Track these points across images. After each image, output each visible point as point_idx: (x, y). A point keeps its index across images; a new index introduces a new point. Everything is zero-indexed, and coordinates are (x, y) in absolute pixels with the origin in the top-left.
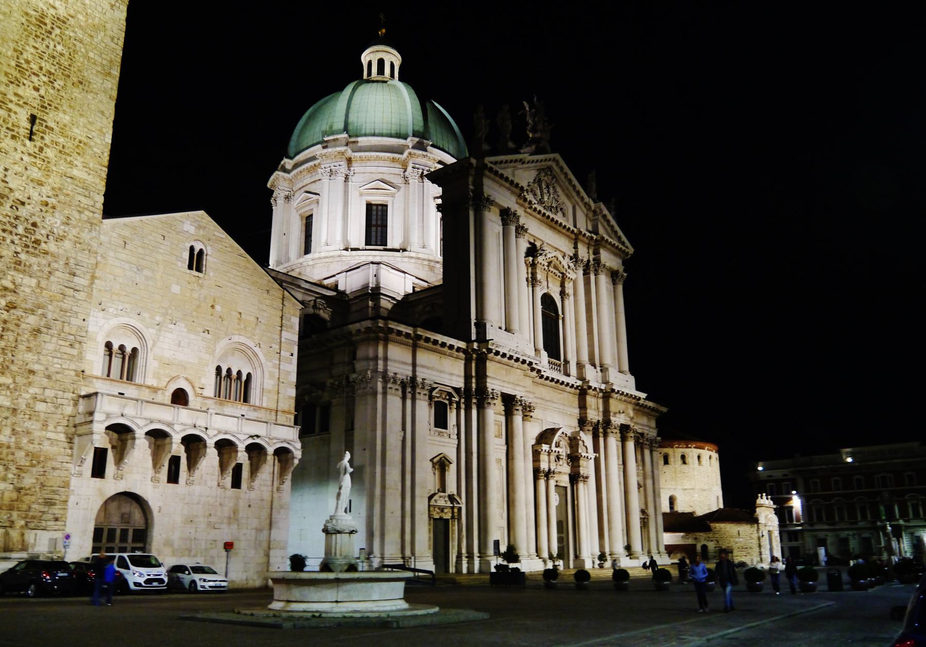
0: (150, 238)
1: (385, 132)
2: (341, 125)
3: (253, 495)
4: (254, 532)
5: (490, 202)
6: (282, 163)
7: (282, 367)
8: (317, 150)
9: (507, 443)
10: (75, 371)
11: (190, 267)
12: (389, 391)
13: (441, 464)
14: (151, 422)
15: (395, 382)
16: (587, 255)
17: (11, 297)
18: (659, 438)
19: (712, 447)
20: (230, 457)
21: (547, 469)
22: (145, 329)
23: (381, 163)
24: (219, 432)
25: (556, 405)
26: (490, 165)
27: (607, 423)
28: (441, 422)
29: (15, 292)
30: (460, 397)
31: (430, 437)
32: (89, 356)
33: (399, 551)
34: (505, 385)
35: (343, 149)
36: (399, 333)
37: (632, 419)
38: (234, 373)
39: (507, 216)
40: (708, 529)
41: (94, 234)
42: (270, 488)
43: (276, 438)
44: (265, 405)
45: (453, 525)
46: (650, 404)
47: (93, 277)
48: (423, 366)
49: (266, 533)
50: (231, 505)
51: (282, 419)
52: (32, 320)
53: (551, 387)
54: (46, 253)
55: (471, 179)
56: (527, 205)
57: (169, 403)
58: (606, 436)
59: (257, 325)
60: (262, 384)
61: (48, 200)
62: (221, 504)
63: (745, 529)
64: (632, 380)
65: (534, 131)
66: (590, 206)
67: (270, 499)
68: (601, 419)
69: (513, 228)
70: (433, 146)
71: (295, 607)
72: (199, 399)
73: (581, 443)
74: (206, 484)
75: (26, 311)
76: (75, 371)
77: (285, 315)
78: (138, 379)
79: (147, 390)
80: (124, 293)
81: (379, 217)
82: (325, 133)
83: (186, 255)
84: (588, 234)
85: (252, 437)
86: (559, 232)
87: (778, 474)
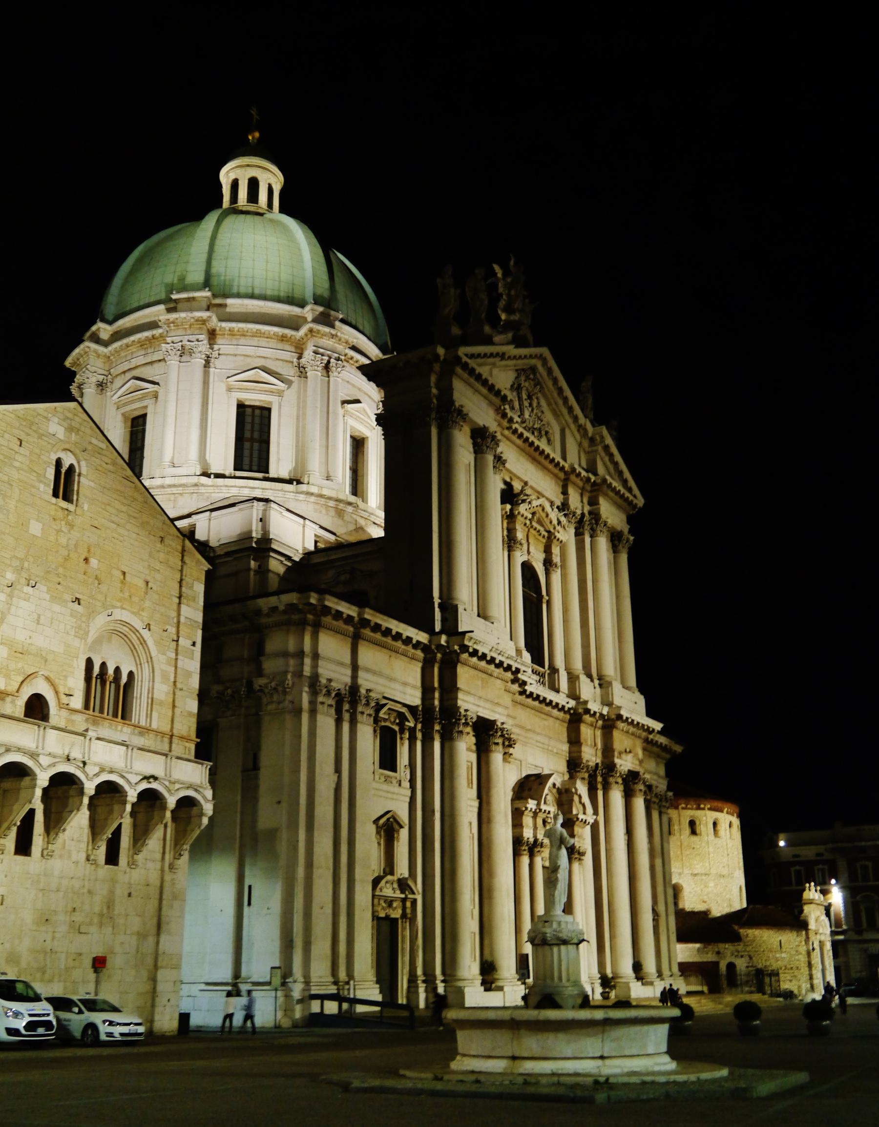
1: (269, 293)
2: (196, 275)
3: (136, 875)
4: (135, 938)
5: (462, 415)
6: (94, 328)
7: (180, 664)
8: (158, 312)
9: (479, 796)
11: (55, 494)
12: (320, 707)
13: (388, 828)
14: (8, 750)
15: (328, 693)
16: (579, 505)
18: (670, 794)
19: (735, 809)
20: (111, 812)
21: (532, 840)
23: (263, 342)
24: (102, 770)
25: (539, 738)
26: (465, 359)
27: (609, 767)
28: (388, 761)
30: (416, 720)
31: (375, 785)
33: (329, 971)
34: (482, 703)
35: (204, 315)
36: (338, 615)
37: (641, 762)
38: (111, 671)
39: (482, 439)
40: (736, 938)
42: (158, 865)
44: (154, 726)
45: (404, 929)
46: (662, 740)
48: (367, 670)
49: (151, 940)
50: (105, 892)
51: (178, 748)
53: (533, 709)
55: (433, 379)
56: (505, 423)
57: (22, 716)
58: (606, 788)
59: (146, 593)
60: (151, 690)
62: (90, 892)
63: (789, 938)
64: (641, 700)
65: (509, 310)
66: (586, 430)
67: (158, 884)
68: (599, 761)
69: (490, 458)
70: (343, 321)
71: (530, 1067)
72: (64, 713)
73: (576, 798)
74: (70, 857)
77: (187, 579)
81: (257, 427)
82: (170, 289)
83: (51, 473)
84: (584, 473)
85: (146, 778)
86: (544, 468)
87: (808, 853)
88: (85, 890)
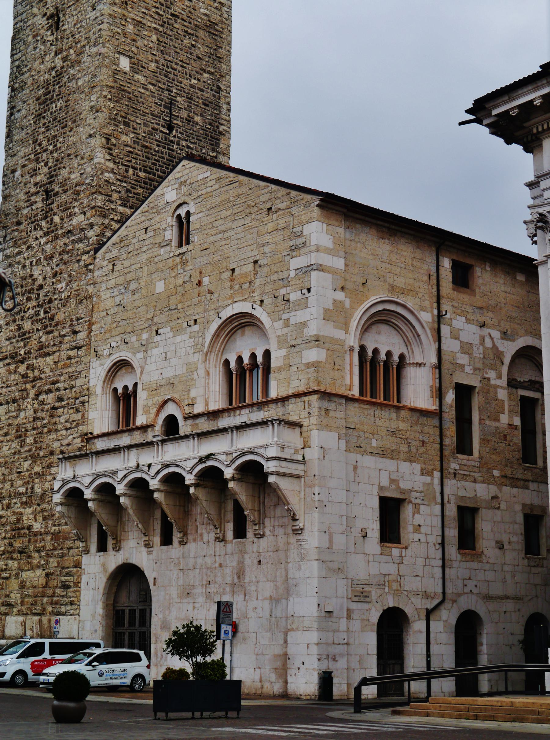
0: (134, 241)
4: (267, 604)
32: (92, 415)
50: (234, 564)
52: (50, 398)
54: (58, 324)
62: (220, 565)
80: (115, 325)
88: (217, 565)
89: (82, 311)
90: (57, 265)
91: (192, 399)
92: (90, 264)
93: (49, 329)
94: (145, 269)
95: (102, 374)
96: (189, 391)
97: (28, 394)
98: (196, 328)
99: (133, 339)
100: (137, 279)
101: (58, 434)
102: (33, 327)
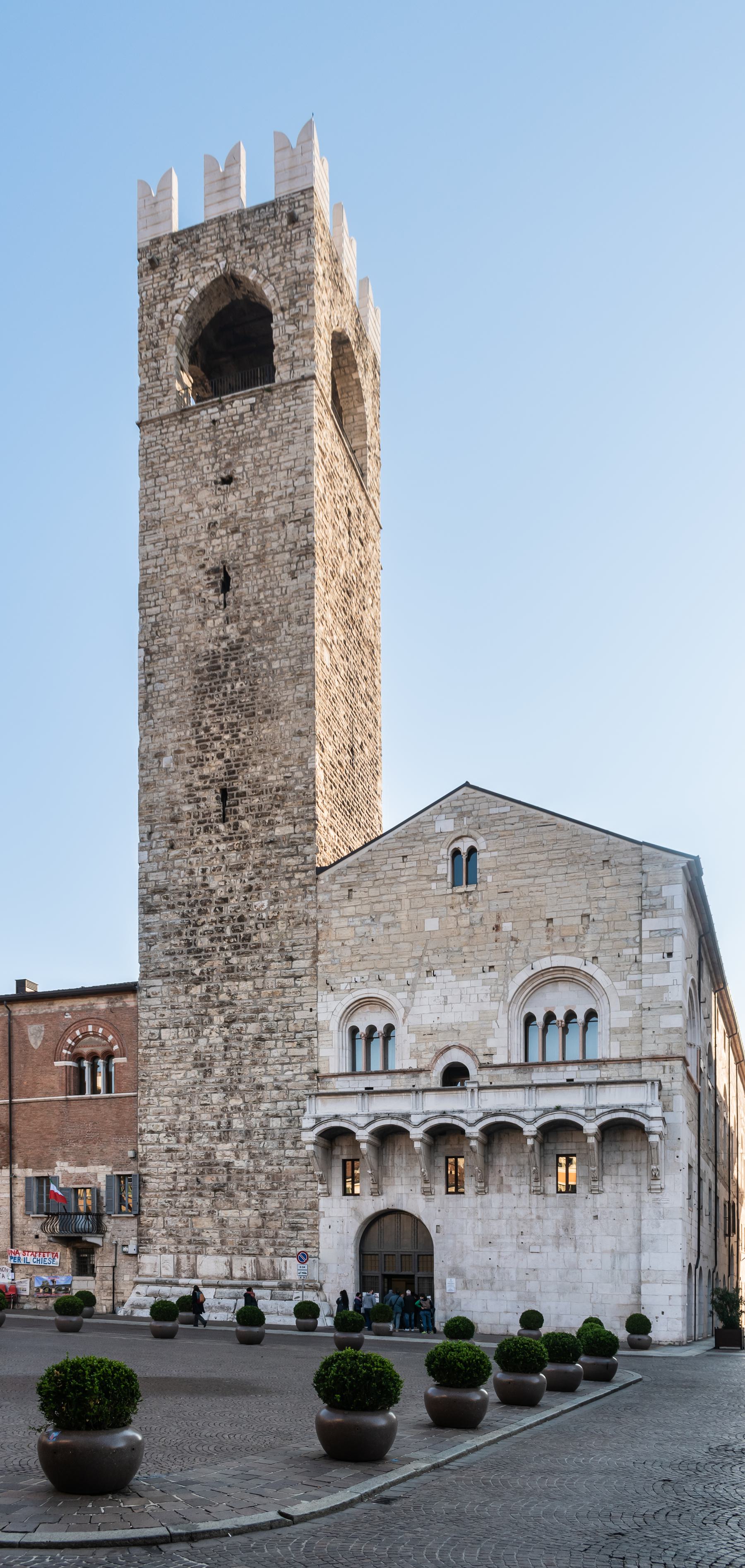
0: (385, 868)
10: (307, 1073)
17: (229, 1011)
22: (391, 997)
29: (232, 1004)
41: (309, 898)
43: (603, 1107)
47: (316, 954)
52: (252, 1028)
54: (258, 946)
57: (439, 1086)
61: (252, 883)
75: (245, 1021)
76: (307, 1073)
78: (395, 1064)
79: (403, 1077)
83: (445, 868)
89: (299, 934)
90: (251, 879)
91: (490, 1049)
92: (311, 885)
93: (242, 950)
94: (406, 902)
95: (338, 1009)
96: (484, 1041)
97: (211, 1021)
98: (493, 975)
99: (391, 977)
100: (393, 913)
101: (269, 1068)
102: (213, 944)
